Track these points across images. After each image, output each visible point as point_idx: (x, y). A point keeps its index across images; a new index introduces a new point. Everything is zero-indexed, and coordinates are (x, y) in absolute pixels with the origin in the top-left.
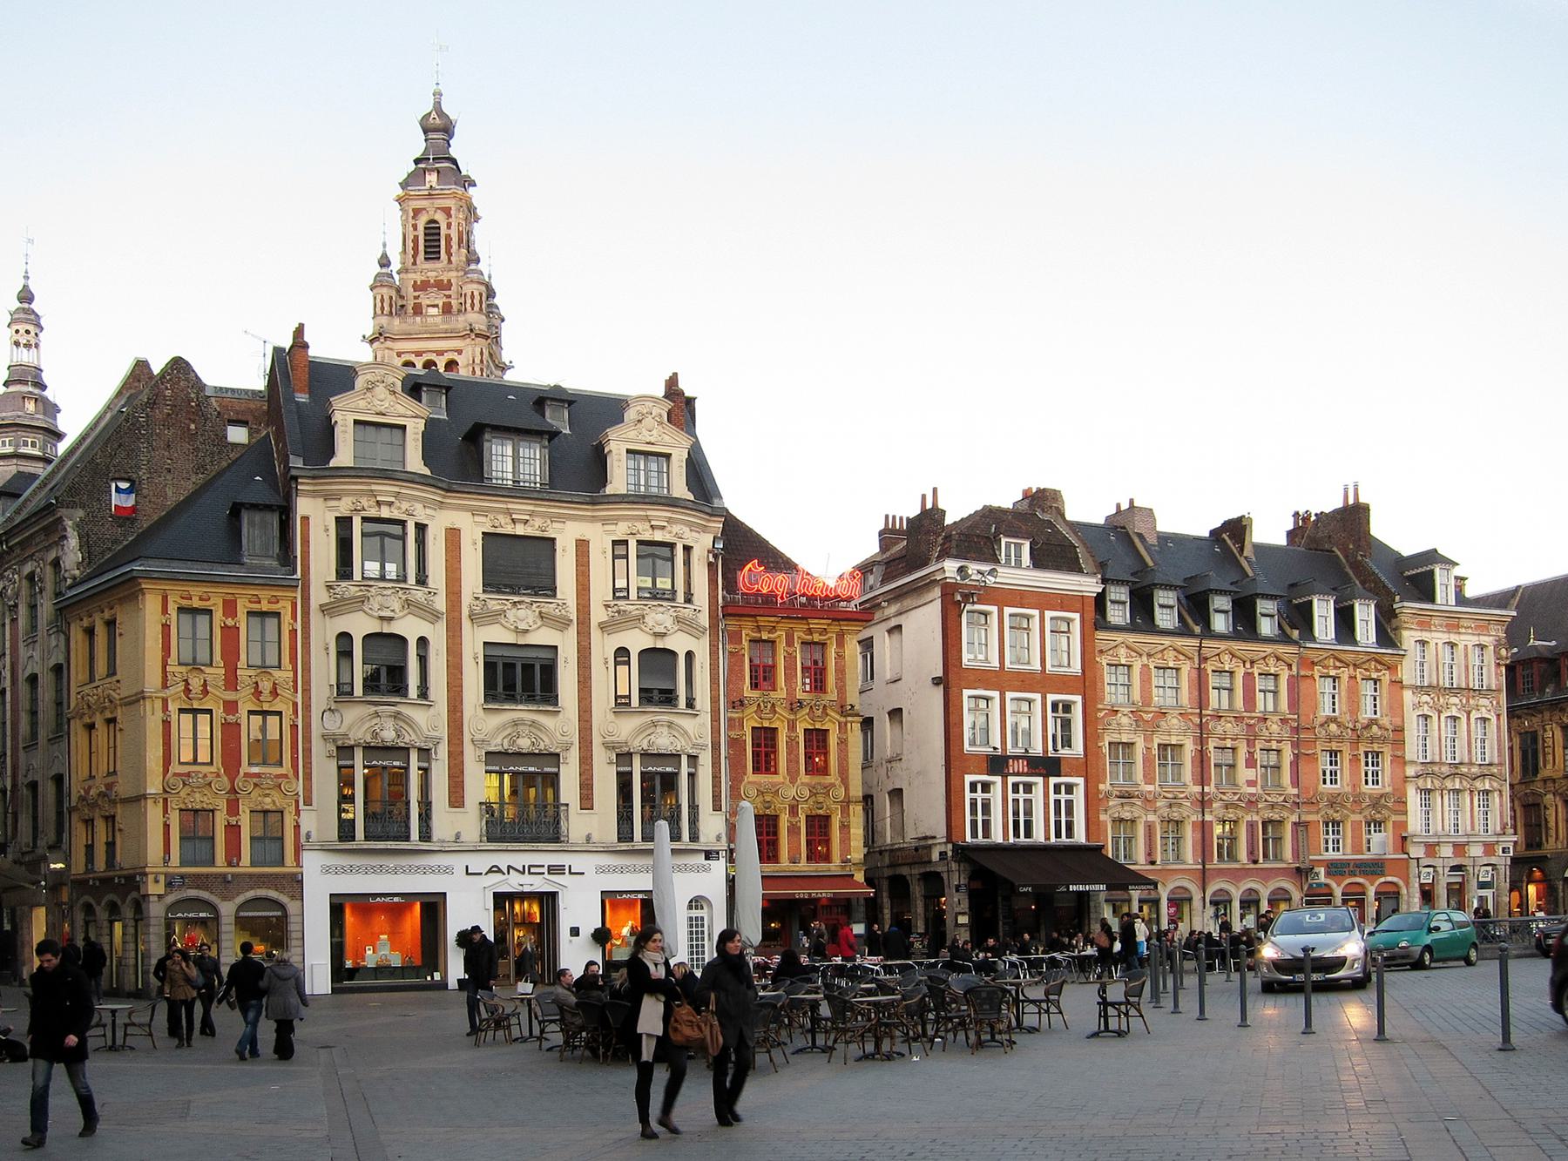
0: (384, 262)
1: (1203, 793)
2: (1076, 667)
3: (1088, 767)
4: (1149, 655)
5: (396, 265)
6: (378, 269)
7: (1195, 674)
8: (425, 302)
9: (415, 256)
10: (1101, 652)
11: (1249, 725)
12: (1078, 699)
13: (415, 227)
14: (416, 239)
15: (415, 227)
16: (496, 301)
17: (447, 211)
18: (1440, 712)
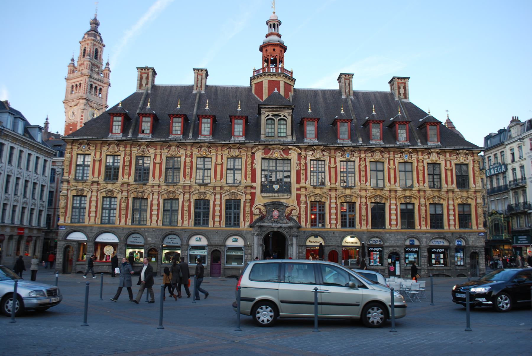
0: (73, 60)
5: (76, 59)
6: (71, 62)
17: (88, 44)
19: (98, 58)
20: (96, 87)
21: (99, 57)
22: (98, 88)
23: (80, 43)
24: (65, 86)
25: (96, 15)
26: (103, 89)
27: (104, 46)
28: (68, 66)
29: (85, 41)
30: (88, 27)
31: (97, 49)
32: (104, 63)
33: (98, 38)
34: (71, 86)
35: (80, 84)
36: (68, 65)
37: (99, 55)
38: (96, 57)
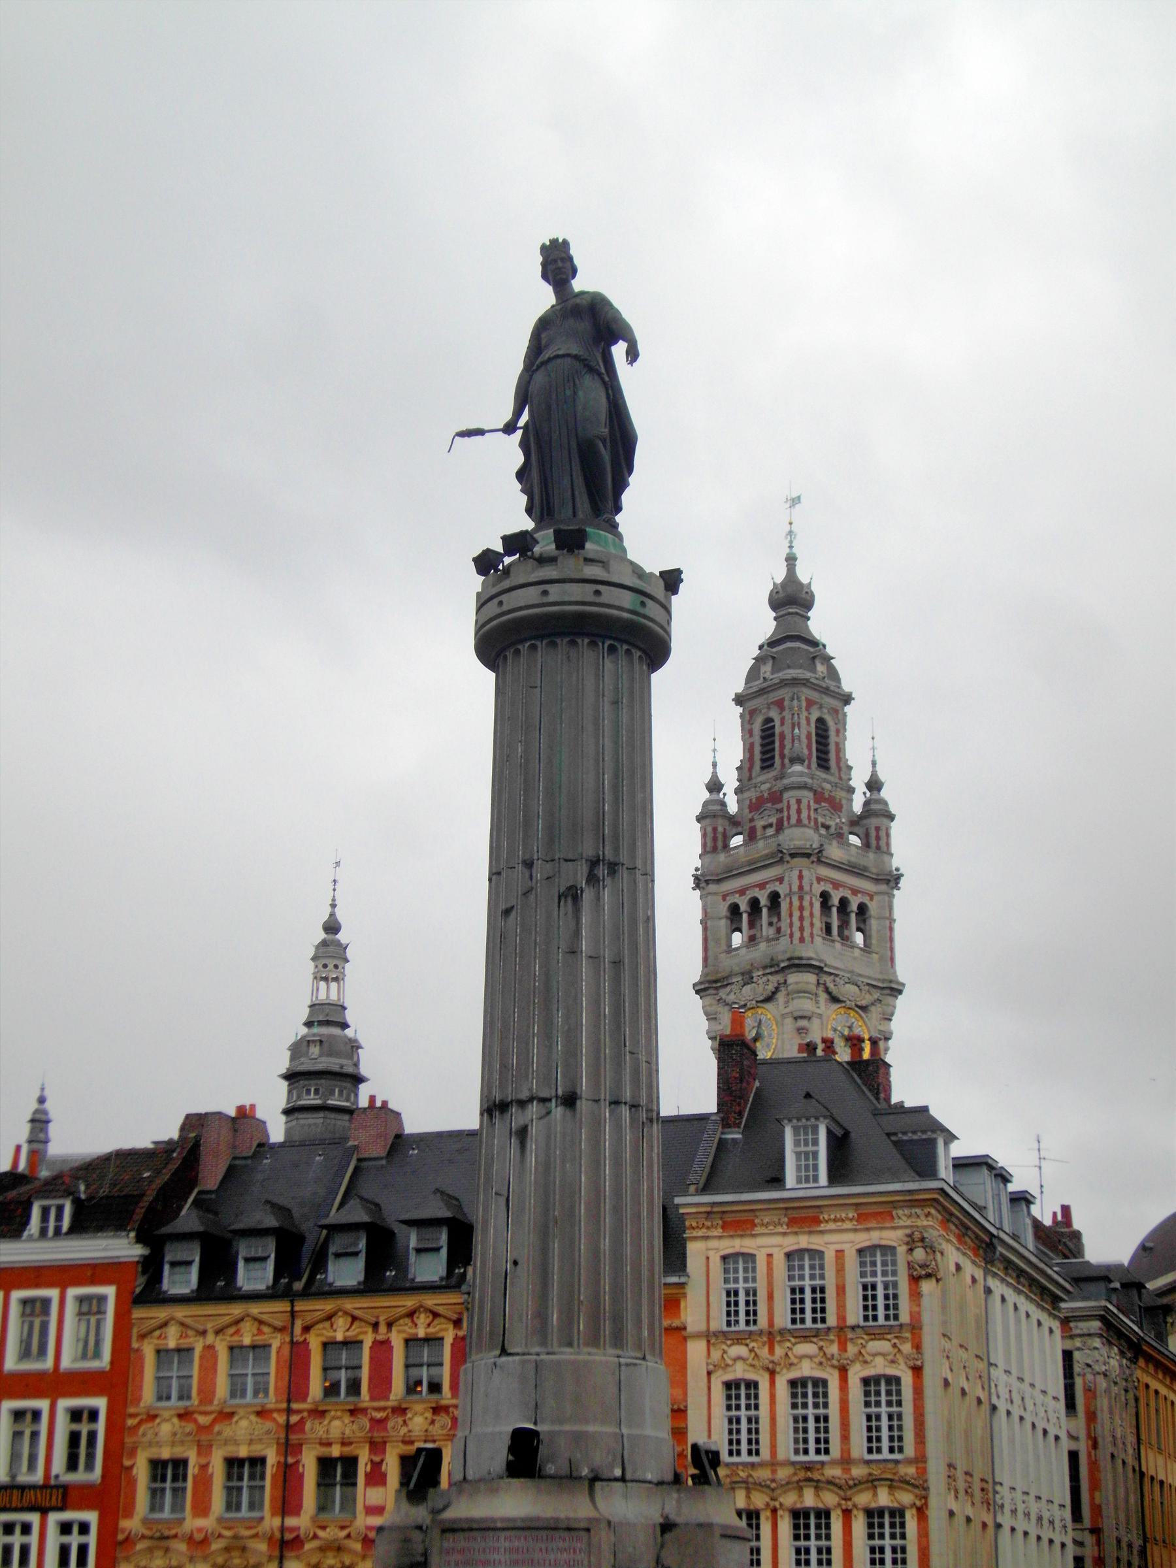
0: (715, 786)
1: (283, 1529)
2: (104, 1361)
3: (109, 1497)
4: (218, 1332)
5: (730, 781)
6: (706, 795)
7: (286, 1350)
8: (760, 824)
9: (750, 769)
10: (143, 1337)
11: (374, 1421)
12: (100, 1403)
13: (751, 733)
14: (752, 745)
15: (751, 733)
16: (884, 794)
17: (780, 704)
18: (772, 1373)
19: (833, 763)
20: (844, 903)
21: (832, 756)
22: (854, 907)
23: (739, 700)
24: (698, 915)
25: (791, 560)
26: (873, 907)
27: (847, 699)
28: (699, 819)
29: (762, 692)
30: (765, 624)
31: (821, 721)
32: (859, 781)
33: (821, 668)
34: (723, 909)
35: (775, 898)
36: (698, 810)
37: (832, 748)
38: (823, 763)
